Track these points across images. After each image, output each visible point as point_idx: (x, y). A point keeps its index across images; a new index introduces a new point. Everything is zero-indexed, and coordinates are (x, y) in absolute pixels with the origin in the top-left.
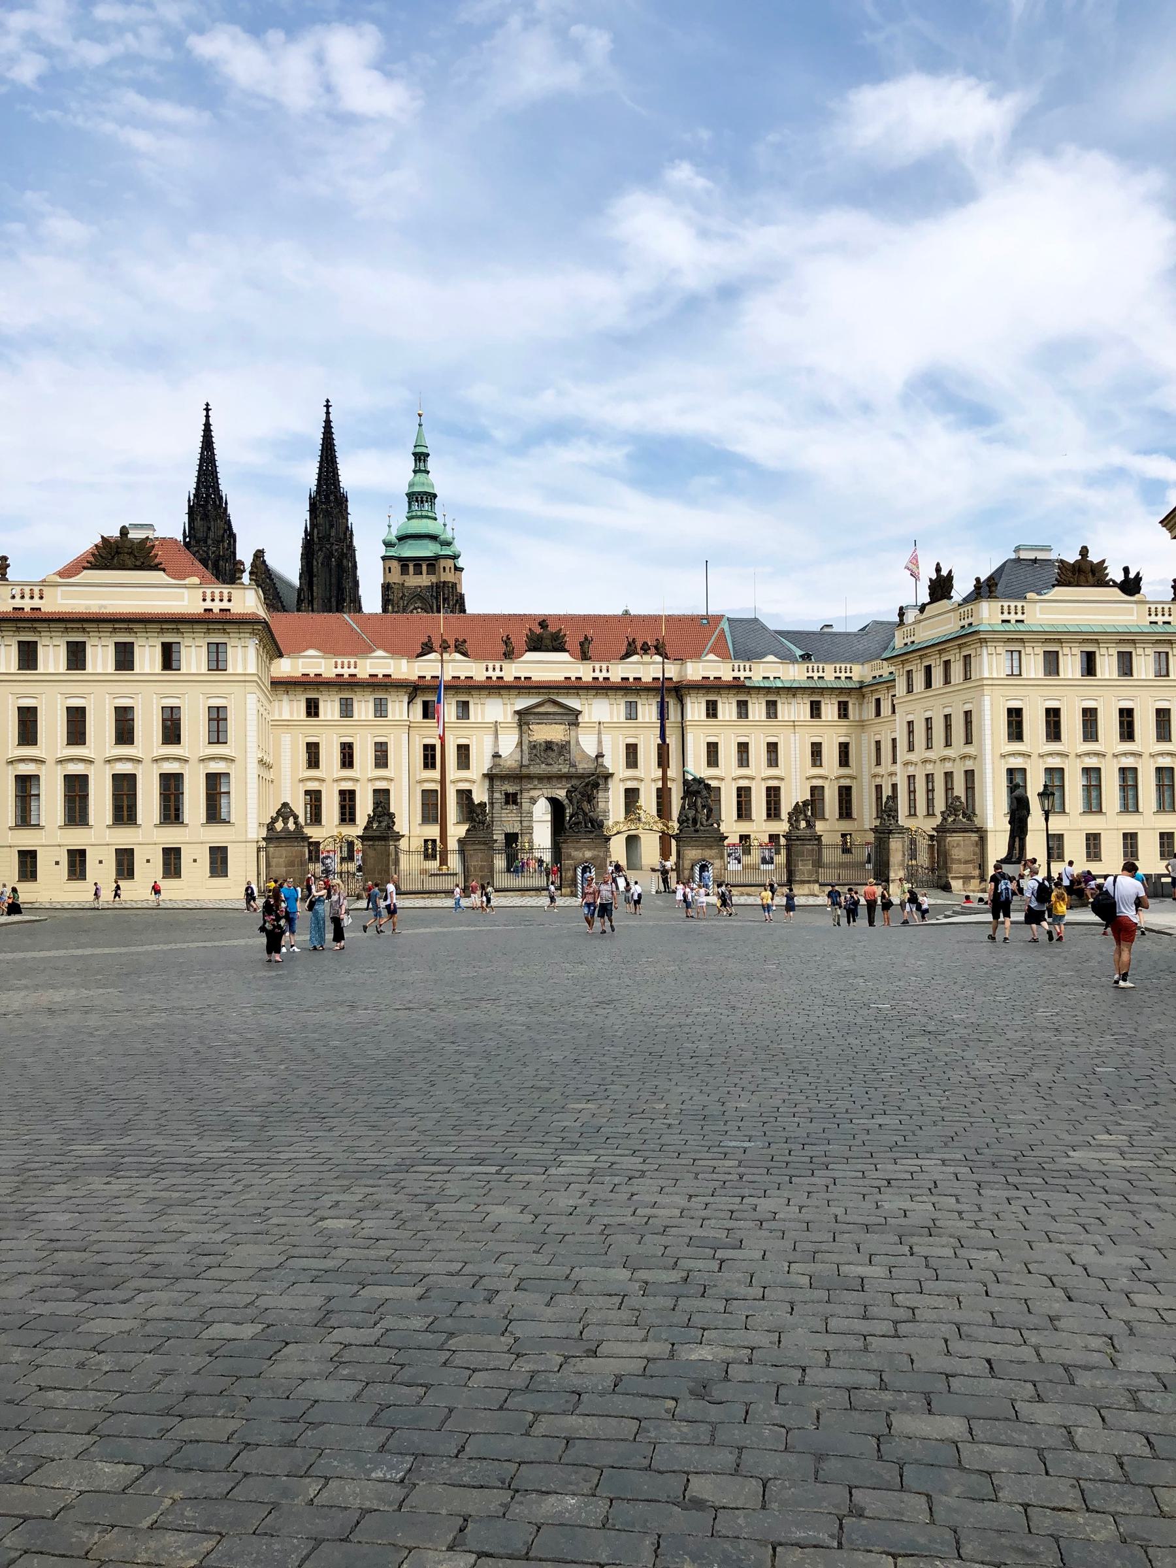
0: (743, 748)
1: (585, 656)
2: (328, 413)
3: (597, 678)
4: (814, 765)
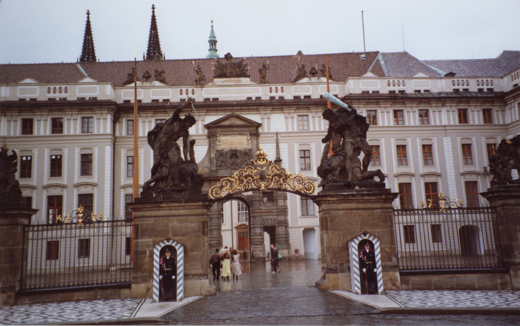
0: (402, 149)
1: (263, 80)
2: (153, 12)
4: (466, 163)
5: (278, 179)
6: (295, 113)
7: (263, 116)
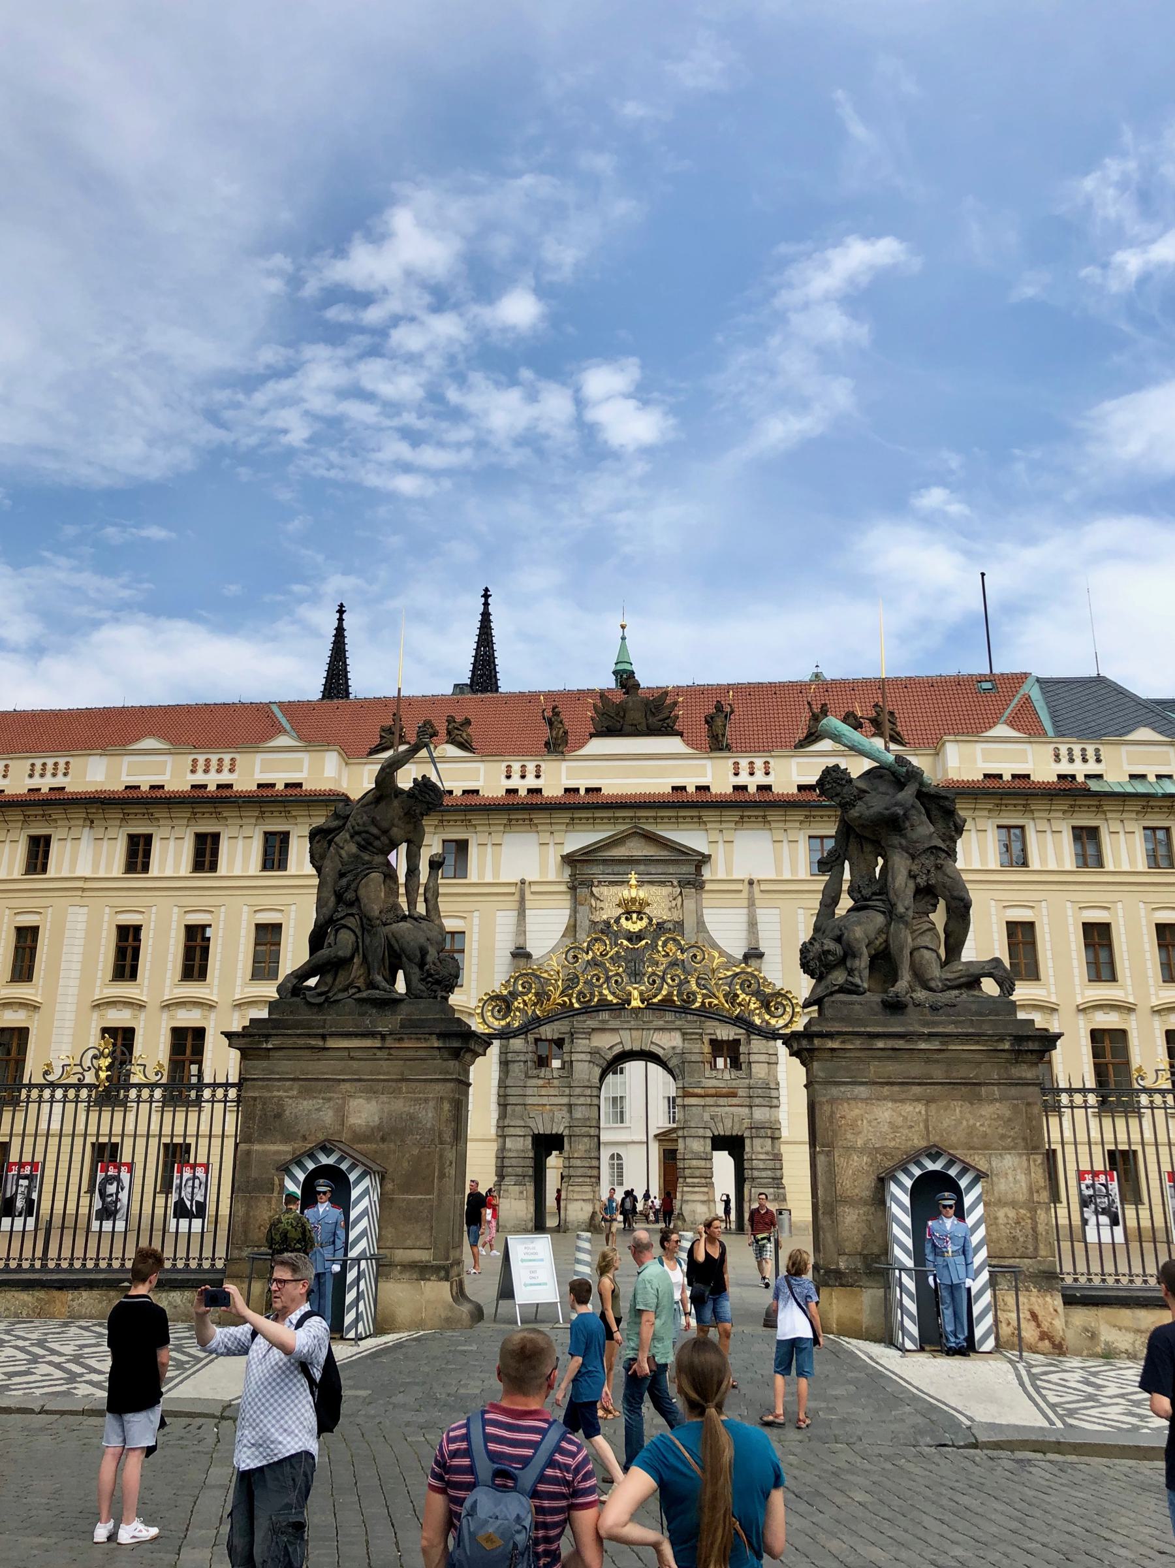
2: (486, 604)
3: (745, 788)
5: (682, 977)
6: (800, 829)
7: (715, 835)
